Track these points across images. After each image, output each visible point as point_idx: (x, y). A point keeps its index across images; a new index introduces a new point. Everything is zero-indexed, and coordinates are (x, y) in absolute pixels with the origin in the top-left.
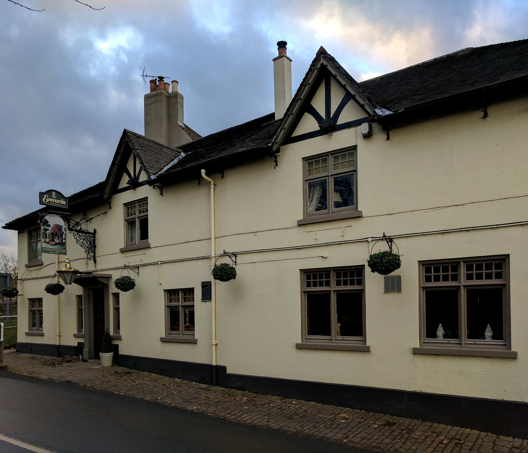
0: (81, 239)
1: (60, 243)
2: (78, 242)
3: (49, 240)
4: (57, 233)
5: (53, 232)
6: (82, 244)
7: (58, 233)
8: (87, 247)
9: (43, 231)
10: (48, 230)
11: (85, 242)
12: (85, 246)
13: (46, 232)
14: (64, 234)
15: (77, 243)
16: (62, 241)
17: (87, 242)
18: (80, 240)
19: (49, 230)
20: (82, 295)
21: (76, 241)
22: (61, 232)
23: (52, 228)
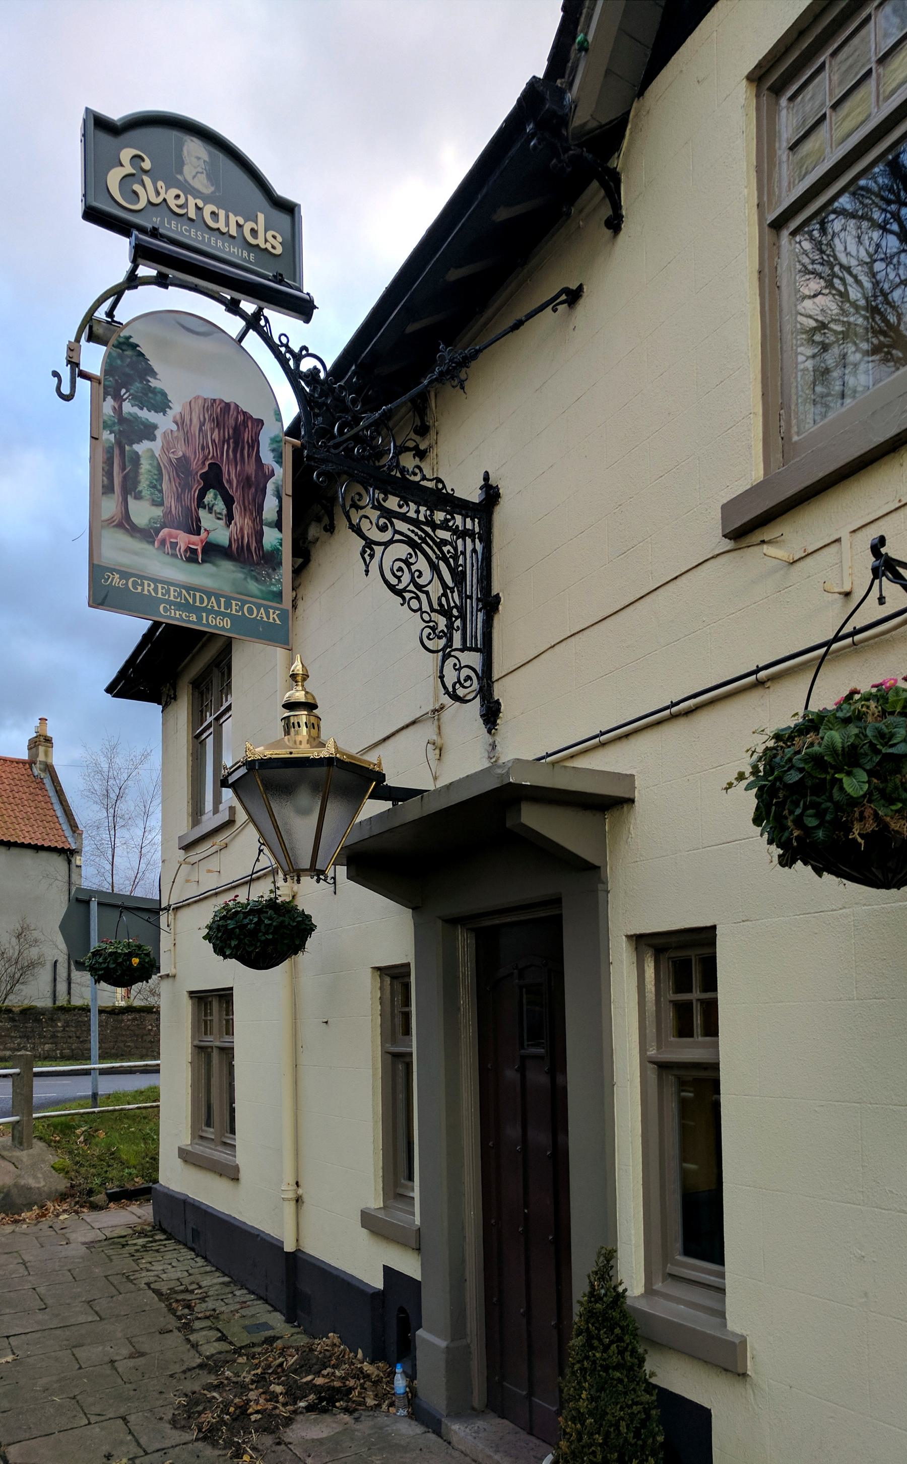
0: (391, 542)
1: (240, 548)
2: (372, 556)
3: (158, 512)
4: (215, 468)
5: (190, 454)
6: (406, 578)
7: (230, 474)
8: (440, 605)
9: (112, 437)
10: (153, 438)
11: (421, 564)
12: (423, 597)
13: (136, 447)
14: (270, 487)
15: (367, 566)
16: (260, 535)
17: (434, 568)
18: (386, 544)
19: (158, 433)
20: (408, 965)
21: (363, 553)
22: (251, 469)
23: (180, 423)
